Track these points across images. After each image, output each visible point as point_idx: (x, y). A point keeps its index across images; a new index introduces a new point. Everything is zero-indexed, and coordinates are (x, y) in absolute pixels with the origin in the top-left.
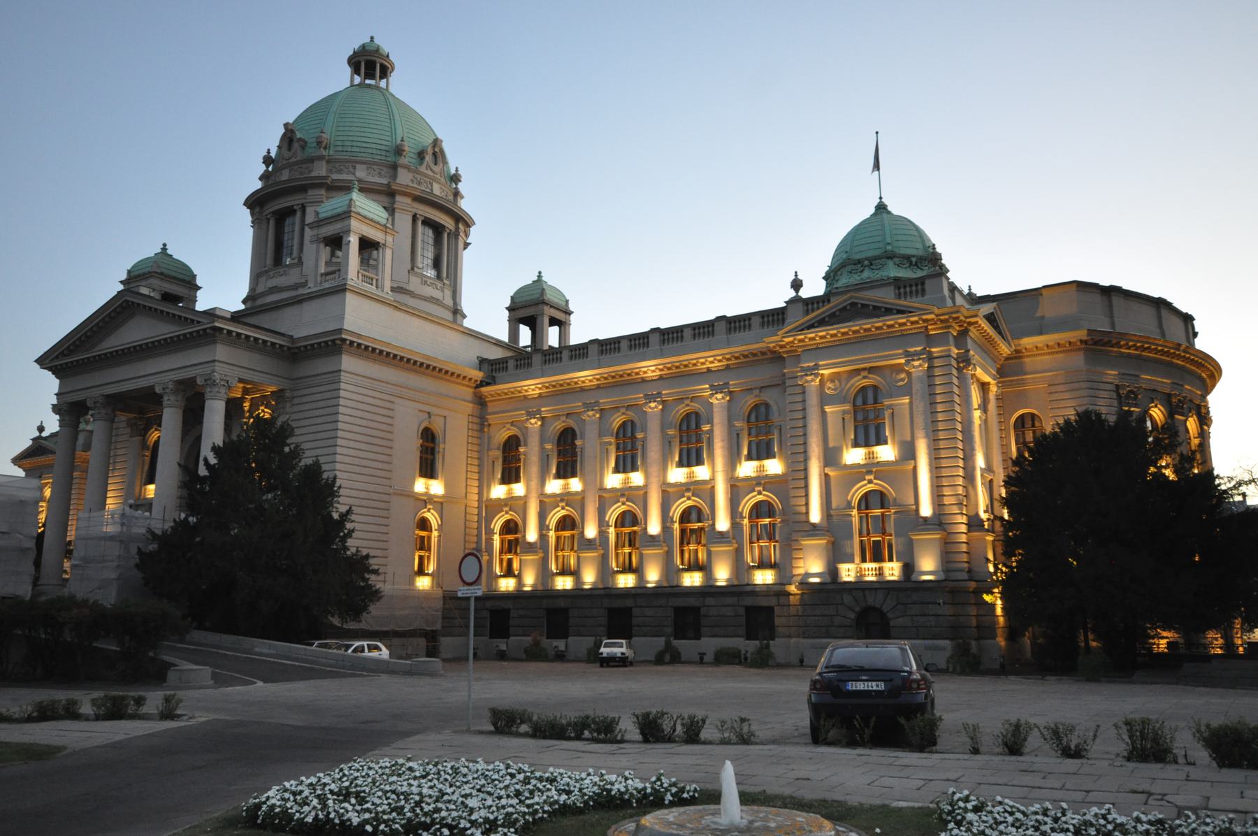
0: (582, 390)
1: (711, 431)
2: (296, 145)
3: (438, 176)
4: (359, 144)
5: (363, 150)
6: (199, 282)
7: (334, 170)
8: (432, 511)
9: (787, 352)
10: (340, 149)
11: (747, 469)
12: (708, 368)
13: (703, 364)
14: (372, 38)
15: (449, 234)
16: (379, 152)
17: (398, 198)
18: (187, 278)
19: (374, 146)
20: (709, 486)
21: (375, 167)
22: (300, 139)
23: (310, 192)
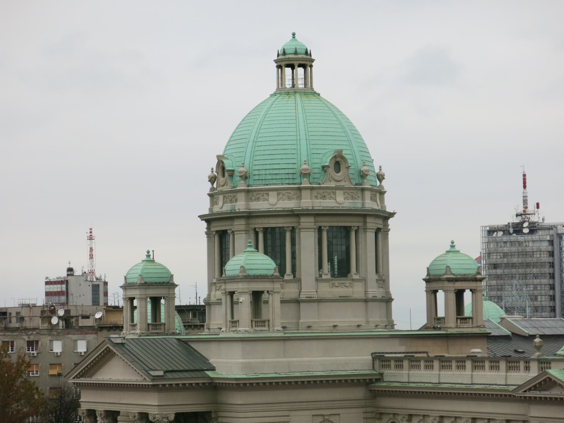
2: (226, 174)
3: (342, 184)
4: (272, 172)
5: (274, 177)
7: (253, 198)
10: (257, 177)
15: (357, 232)
16: (287, 176)
17: (303, 219)
18: (166, 280)
19: (283, 171)
21: (284, 192)
22: (229, 171)
23: (237, 222)
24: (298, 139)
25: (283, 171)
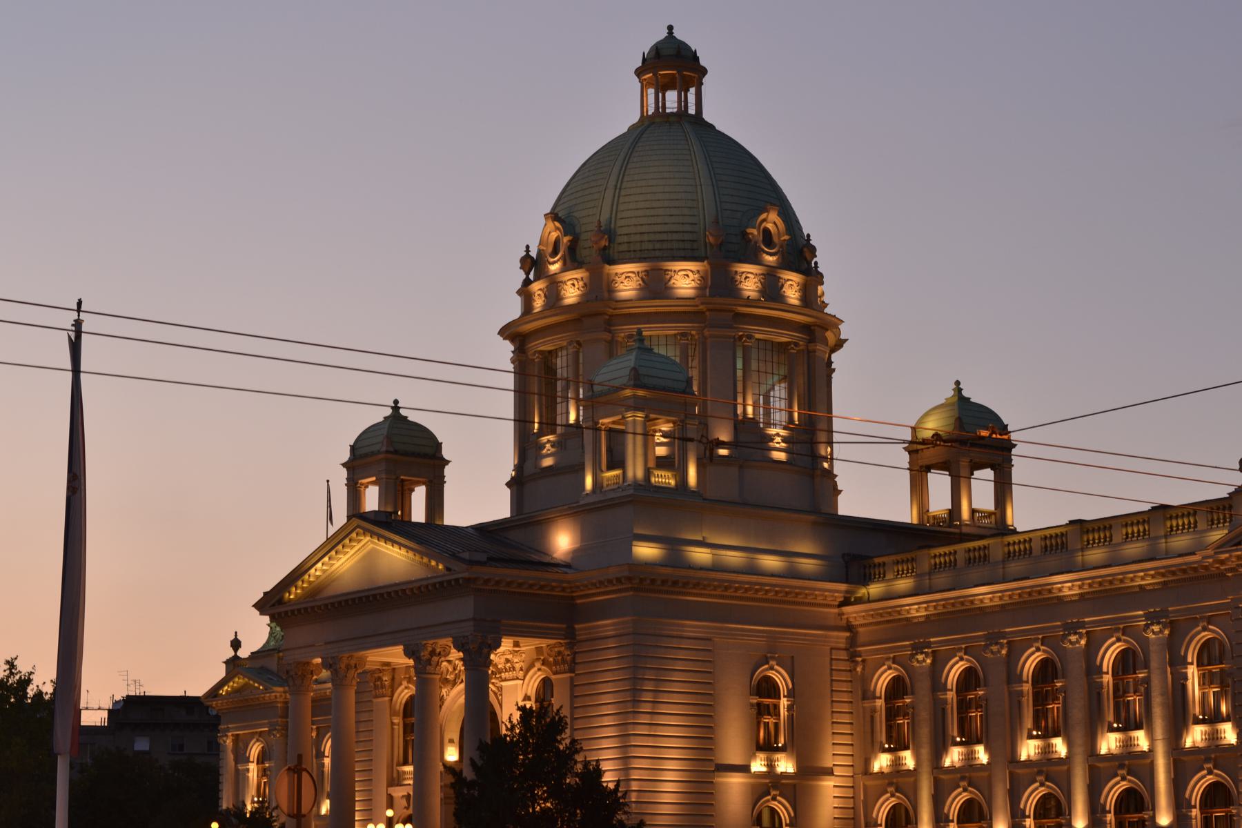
0: (983, 611)
1: (1147, 681)
6: (446, 454)
8: (778, 798)
9: (1231, 570)
11: (1195, 736)
12: (1140, 586)
13: (1132, 580)
14: (670, 28)
20: (1149, 761)
24: (698, 183)
25: (675, 237)
